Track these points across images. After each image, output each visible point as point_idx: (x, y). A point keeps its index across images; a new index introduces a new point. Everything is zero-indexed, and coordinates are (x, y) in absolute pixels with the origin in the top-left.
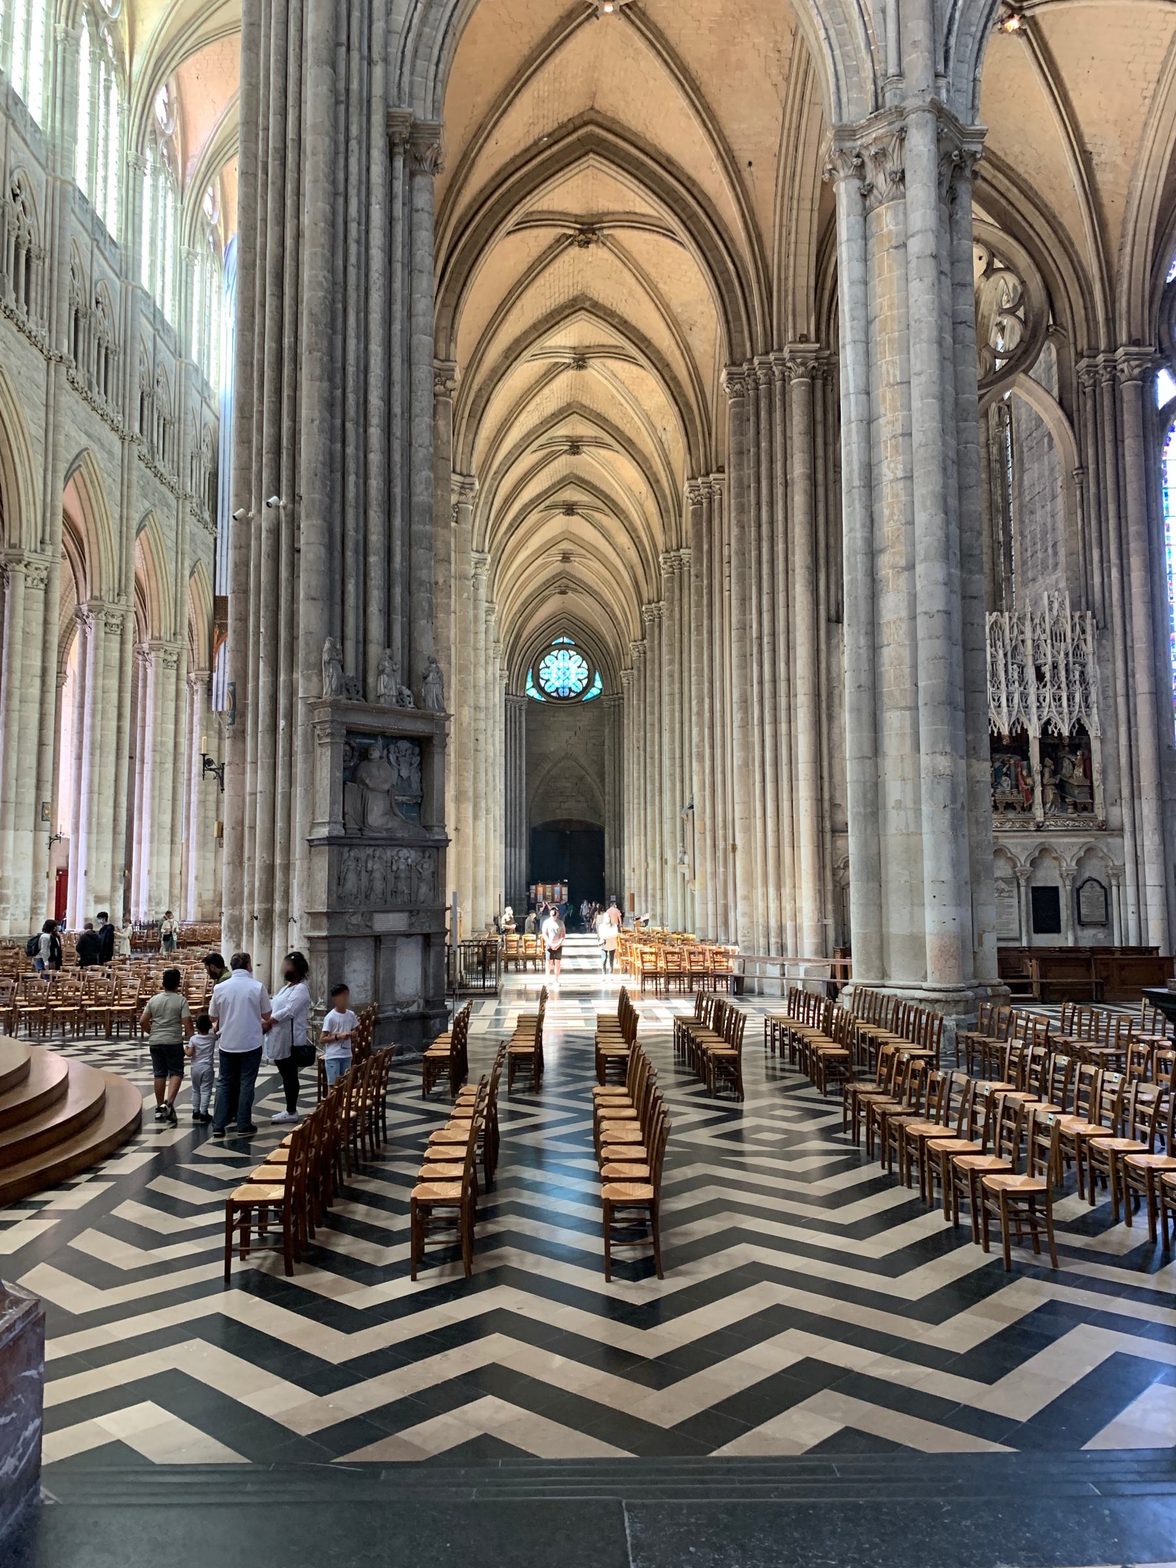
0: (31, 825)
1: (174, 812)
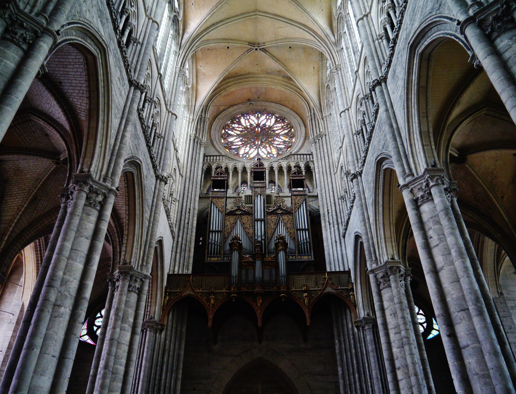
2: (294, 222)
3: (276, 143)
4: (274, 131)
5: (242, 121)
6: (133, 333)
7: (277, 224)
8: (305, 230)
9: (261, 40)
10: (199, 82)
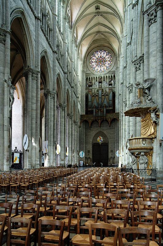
0: (52, 145)
1: (72, 145)
2: (109, 98)
3: (106, 64)
4: (106, 59)
5: (96, 55)
6: (77, 133)
7: (104, 99)
8: (111, 100)
9: (101, 31)
10: (82, 47)
